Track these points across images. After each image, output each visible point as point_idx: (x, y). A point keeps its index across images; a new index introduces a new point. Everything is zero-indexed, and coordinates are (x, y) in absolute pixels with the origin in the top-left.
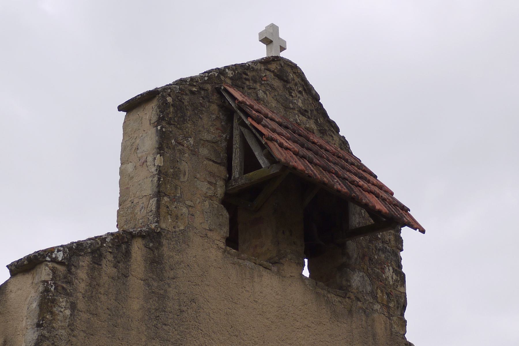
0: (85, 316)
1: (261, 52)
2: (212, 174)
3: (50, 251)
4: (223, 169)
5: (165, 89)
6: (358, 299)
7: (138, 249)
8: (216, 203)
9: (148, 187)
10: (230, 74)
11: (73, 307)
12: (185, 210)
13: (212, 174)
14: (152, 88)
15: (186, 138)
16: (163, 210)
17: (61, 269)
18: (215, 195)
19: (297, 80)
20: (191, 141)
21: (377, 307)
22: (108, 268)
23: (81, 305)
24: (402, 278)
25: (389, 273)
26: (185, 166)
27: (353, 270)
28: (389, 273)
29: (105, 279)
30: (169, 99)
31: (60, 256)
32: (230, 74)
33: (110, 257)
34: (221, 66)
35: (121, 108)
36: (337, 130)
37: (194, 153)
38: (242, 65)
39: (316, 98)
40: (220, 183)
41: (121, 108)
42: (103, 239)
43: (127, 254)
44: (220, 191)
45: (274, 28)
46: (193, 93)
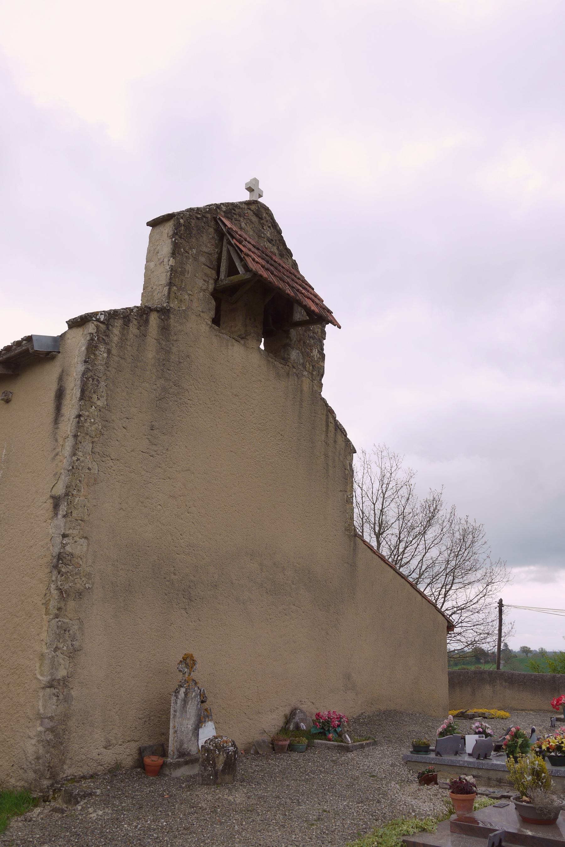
0: (116, 359)
1: (246, 196)
2: (206, 275)
3: (96, 314)
4: (214, 272)
5: (179, 213)
6: (294, 367)
7: (154, 318)
8: (208, 295)
9: (163, 279)
10: (224, 208)
11: (109, 352)
12: (187, 297)
13: (206, 275)
14: (170, 212)
15: (191, 248)
16: (172, 295)
17: (103, 326)
18: (207, 289)
19: (268, 218)
20: (195, 251)
21: (305, 373)
22: (133, 329)
23: (114, 351)
24: (323, 357)
25: (315, 353)
26: (189, 267)
27: (293, 348)
28: (315, 353)
29: (131, 336)
30: (182, 221)
31: (102, 318)
32: (224, 208)
33: (135, 322)
34: (218, 202)
35: (149, 224)
36: (291, 255)
37: (196, 259)
38: (232, 204)
39: (279, 232)
40: (211, 282)
41: (149, 224)
42: (131, 310)
43: (147, 321)
44: (211, 287)
45: (256, 181)
46: (198, 218)
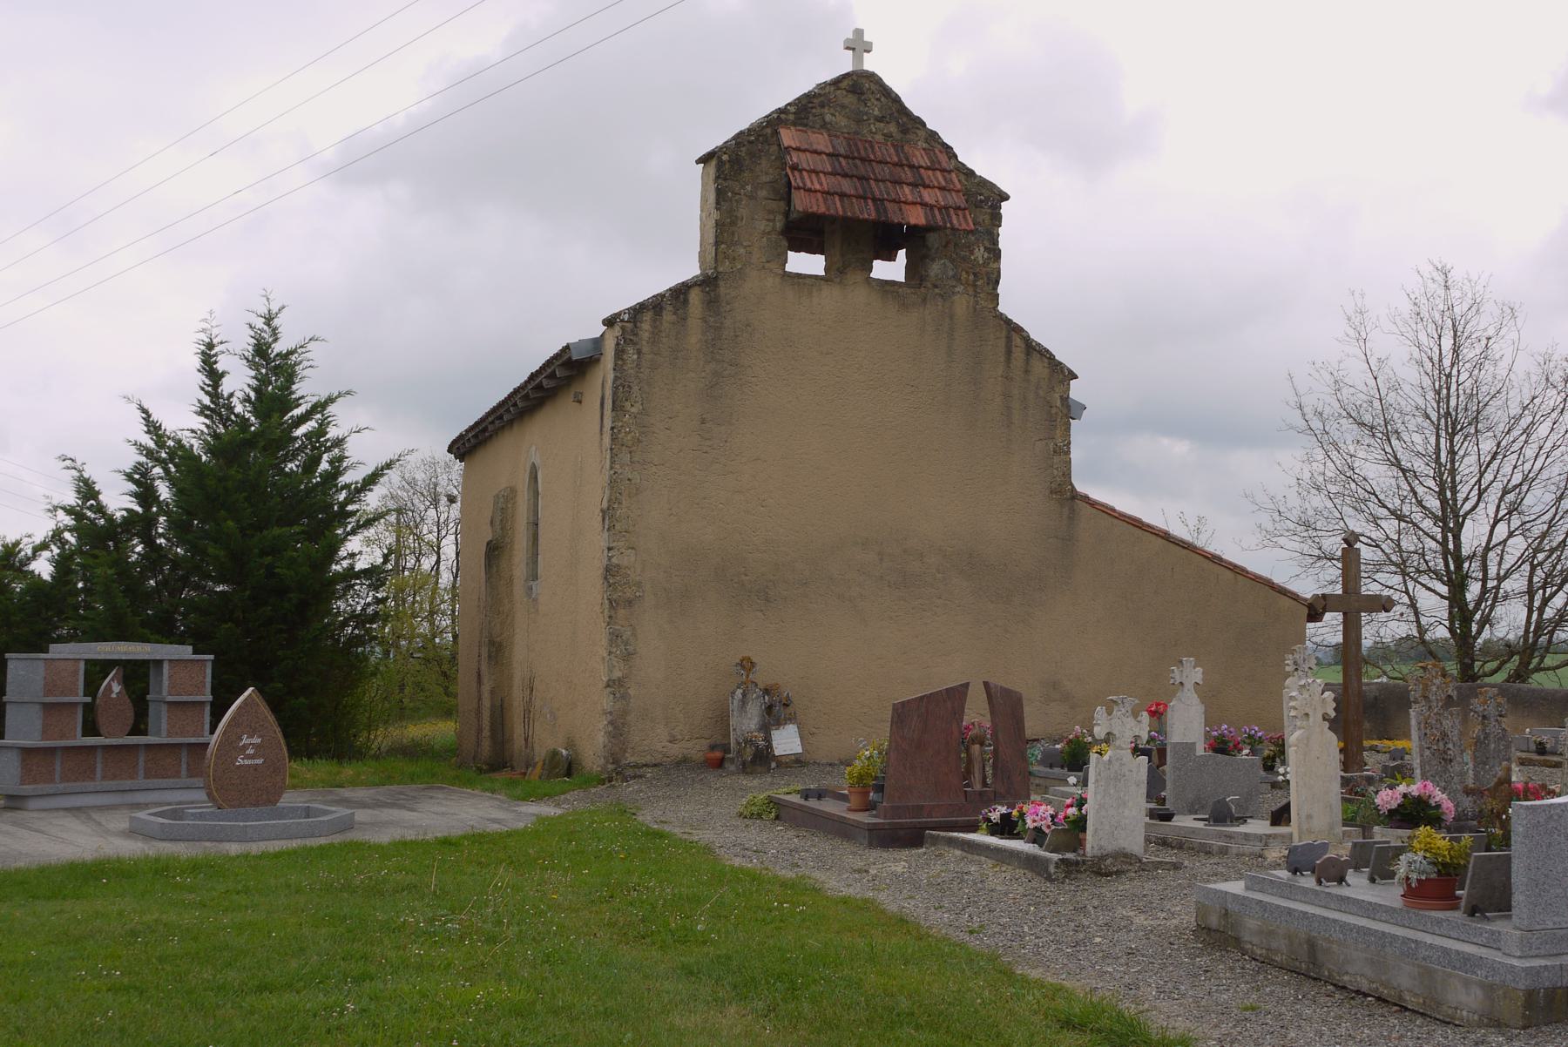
0: (649, 357)
1: (843, 64)
2: (770, 212)
3: (618, 314)
4: (782, 204)
5: (720, 148)
6: (936, 286)
7: (695, 296)
8: (774, 237)
9: (712, 240)
10: (792, 109)
11: (639, 352)
12: (742, 251)
13: (770, 212)
14: (709, 149)
15: (743, 187)
16: (721, 256)
17: (629, 325)
18: (774, 229)
19: (873, 87)
20: (749, 188)
21: (960, 288)
22: (668, 316)
23: (645, 349)
24: (997, 254)
25: (980, 254)
26: (743, 212)
27: (933, 260)
28: (980, 254)
29: (665, 325)
30: (725, 157)
31: (626, 317)
32: (792, 109)
33: (669, 308)
34: (782, 104)
35: (698, 162)
36: (924, 124)
37: (752, 197)
38: (806, 96)
39: (896, 100)
40: (779, 217)
41: (698, 162)
42: (662, 296)
43: (686, 301)
44: (779, 225)
45: (859, 33)
46: (751, 142)
